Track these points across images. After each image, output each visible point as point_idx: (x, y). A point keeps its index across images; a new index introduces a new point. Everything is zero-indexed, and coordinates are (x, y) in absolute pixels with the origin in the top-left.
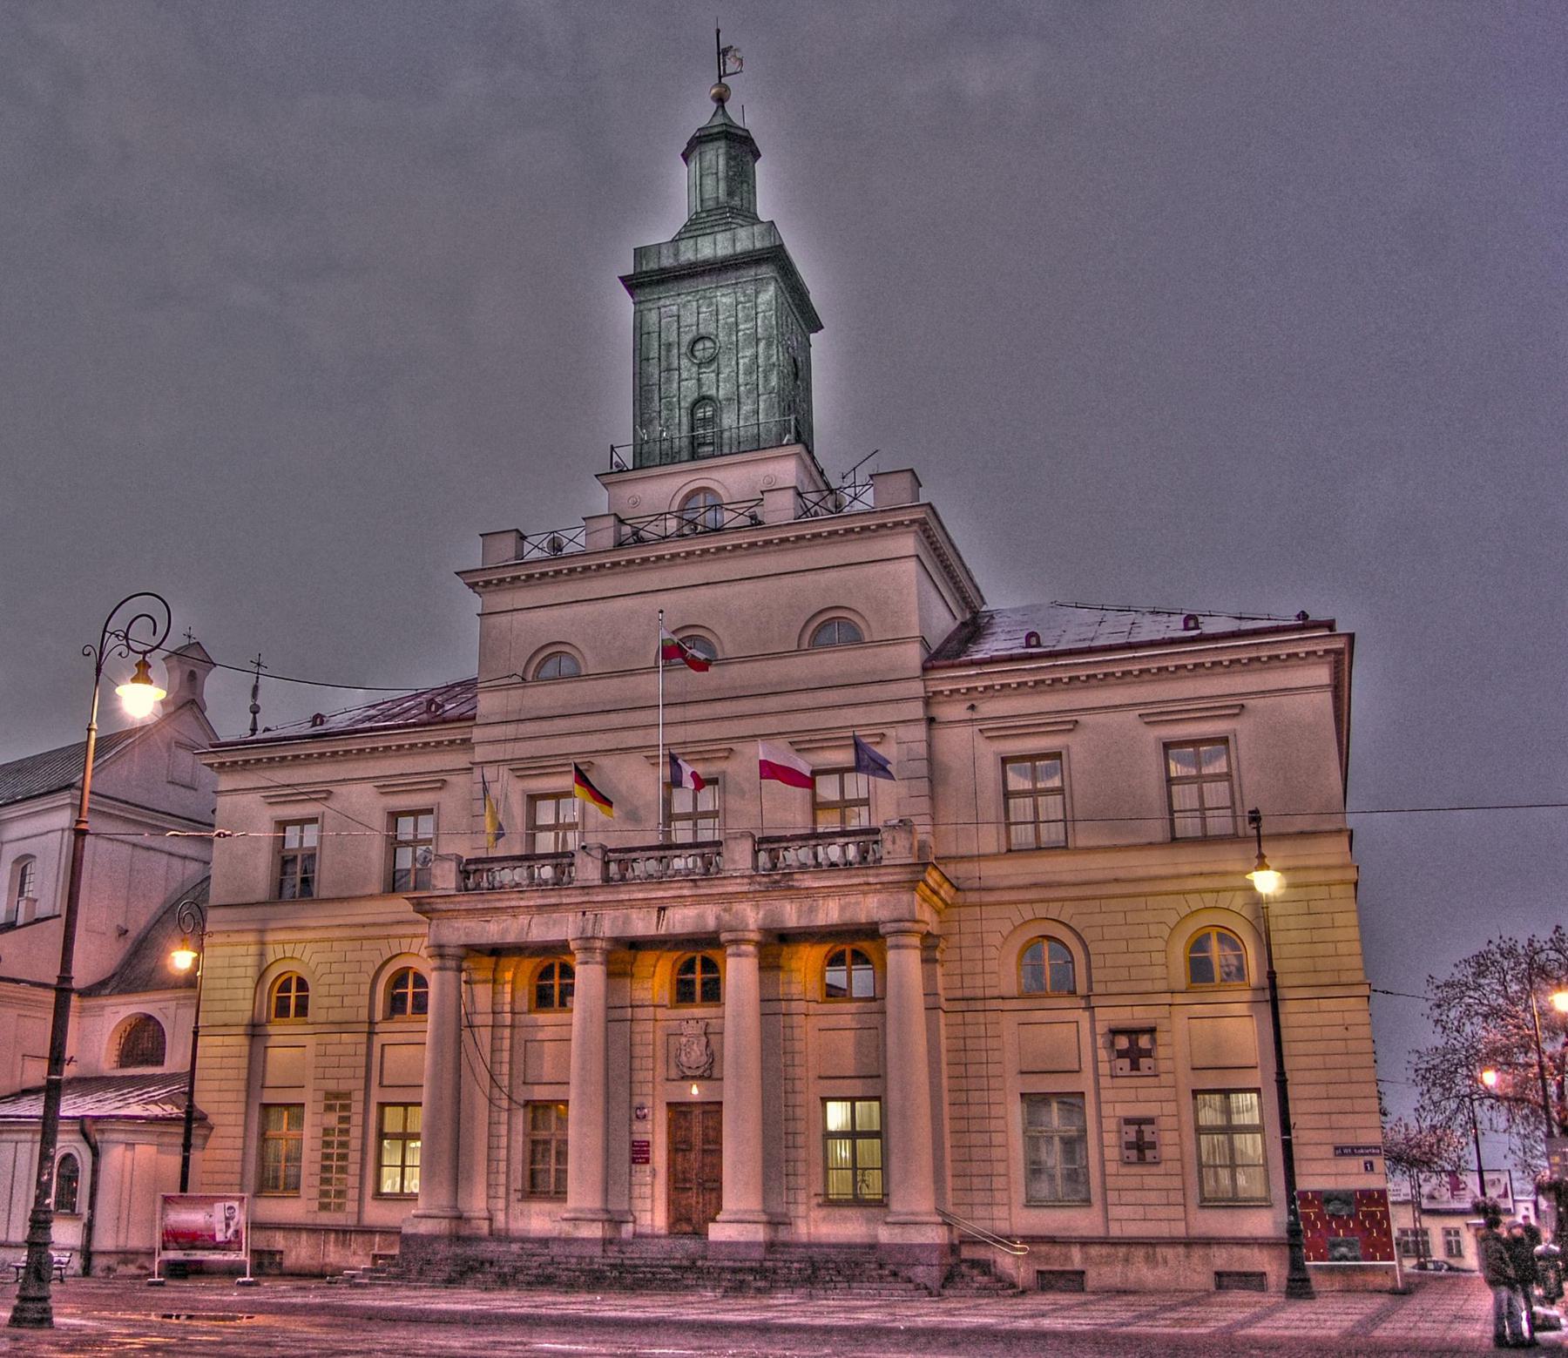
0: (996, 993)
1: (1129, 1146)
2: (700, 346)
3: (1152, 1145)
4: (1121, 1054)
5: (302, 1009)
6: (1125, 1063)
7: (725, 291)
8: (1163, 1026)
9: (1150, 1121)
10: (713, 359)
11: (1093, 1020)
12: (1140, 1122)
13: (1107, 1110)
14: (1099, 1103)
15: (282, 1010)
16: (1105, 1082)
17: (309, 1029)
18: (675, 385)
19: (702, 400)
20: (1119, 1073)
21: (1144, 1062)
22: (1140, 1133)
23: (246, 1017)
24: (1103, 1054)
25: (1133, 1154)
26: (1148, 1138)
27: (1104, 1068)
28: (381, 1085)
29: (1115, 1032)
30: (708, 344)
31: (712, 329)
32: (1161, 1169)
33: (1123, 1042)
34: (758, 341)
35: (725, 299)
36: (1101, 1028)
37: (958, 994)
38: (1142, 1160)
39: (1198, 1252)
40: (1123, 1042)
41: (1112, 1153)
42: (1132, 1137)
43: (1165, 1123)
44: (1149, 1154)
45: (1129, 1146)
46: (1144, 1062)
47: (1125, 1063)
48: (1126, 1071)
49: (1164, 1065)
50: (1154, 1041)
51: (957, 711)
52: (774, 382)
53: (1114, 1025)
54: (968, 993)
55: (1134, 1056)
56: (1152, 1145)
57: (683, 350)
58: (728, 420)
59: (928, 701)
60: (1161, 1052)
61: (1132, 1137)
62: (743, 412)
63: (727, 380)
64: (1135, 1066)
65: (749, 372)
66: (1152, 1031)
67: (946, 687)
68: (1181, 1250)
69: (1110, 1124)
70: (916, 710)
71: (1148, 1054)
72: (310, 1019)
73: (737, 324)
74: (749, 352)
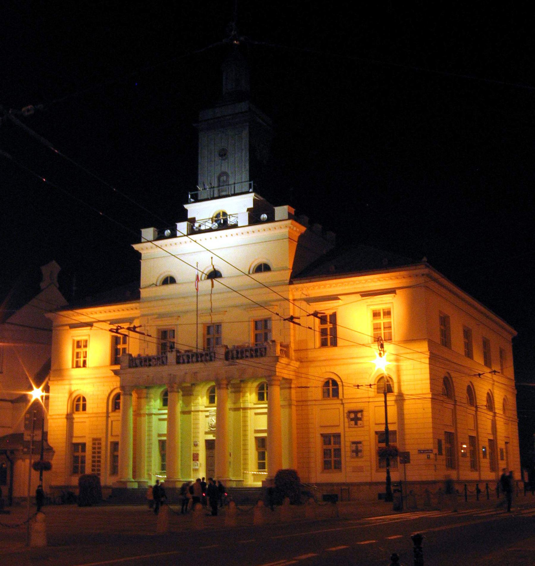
1: (353, 451)
3: (361, 451)
4: (352, 420)
5: (84, 409)
9: (360, 443)
11: (344, 407)
13: (347, 439)
14: (345, 437)
15: (77, 409)
16: (347, 429)
17: (87, 416)
22: (357, 447)
23: (65, 413)
24: (346, 420)
26: (360, 448)
27: (347, 425)
28: (112, 435)
29: (350, 412)
32: (362, 459)
33: (352, 416)
34: (242, 150)
36: (346, 411)
37: (300, 399)
41: (349, 454)
43: (365, 443)
44: (360, 454)
45: (353, 451)
48: (353, 426)
49: (366, 423)
50: (362, 415)
54: (303, 399)
60: (365, 418)
61: (354, 448)
64: (356, 424)
66: (361, 411)
69: (348, 444)
71: (360, 419)
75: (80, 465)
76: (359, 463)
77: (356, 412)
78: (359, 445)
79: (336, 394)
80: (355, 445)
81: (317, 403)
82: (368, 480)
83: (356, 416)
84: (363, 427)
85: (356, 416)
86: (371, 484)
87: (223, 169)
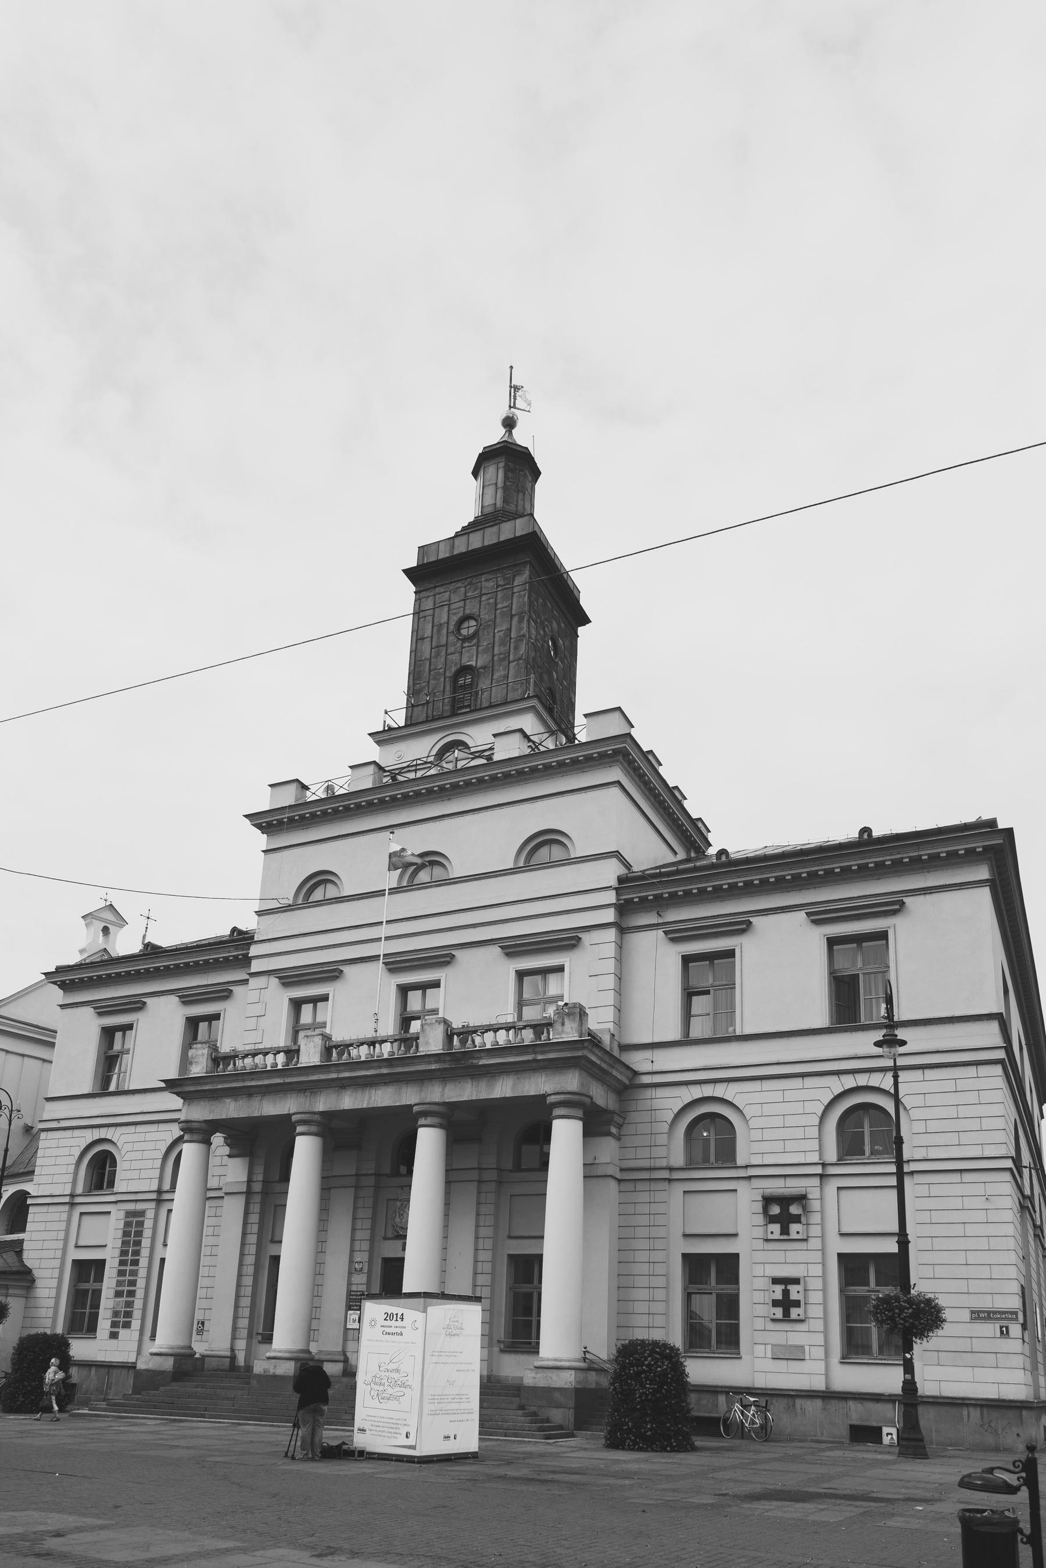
0: (663, 1163)
1: (775, 1303)
2: (466, 625)
3: (797, 1304)
4: (772, 1219)
5: (111, 1184)
6: (776, 1228)
7: (489, 576)
8: (814, 1194)
9: (796, 1281)
10: (475, 634)
12: (786, 1281)
18: (443, 659)
19: (465, 670)
20: (770, 1237)
21: (794, 1228)
22: (786, 1293)
25: (779, 1312)
26: (794, 1296)
29: (768, 1200)
30: (473, 623)
31: (476, 610)
33: (775, 1210)
34: (512, 616)
35: (488, 584)
38: (786, 1317)
39: (834, 1405)
40: (775, 1210)
42: (778, 1296)
44: (794, 1313)
45: (775, 1303)
46: (794, 1228)
47: (776, 1228)
48: (777, 1235)
50: (804, 1208)
51: (651, 919)
52: (522, 650)
53: (768, 1192)
55: (785, 1221)
56: (797, 1304)
57: (451, 627)
58: (484, 684)
62: (495, 677)
63: (485, 651)
64: (785, 1231)
65: (503, 643)
66: (801, 1199)
67: (635, 896)
68: (819, 1403)
69: (764, 1283)
70: (609, 916)
71: (797, 1219)
72: (115, 1190)
73: (496, 604)
74: (505, 626)
75: (87, 1311)
76: (795, 1336)
77: (785, 1201)
78: (793, 1289)
79: (725, 1152)
80: (783, 1287)
81: (676, 1175)
82: (819, 1384)
83: (785, 1209)
84: (805, 1240)
85: (785, 1209)
86: (828, 1396)
87: (465, 661)
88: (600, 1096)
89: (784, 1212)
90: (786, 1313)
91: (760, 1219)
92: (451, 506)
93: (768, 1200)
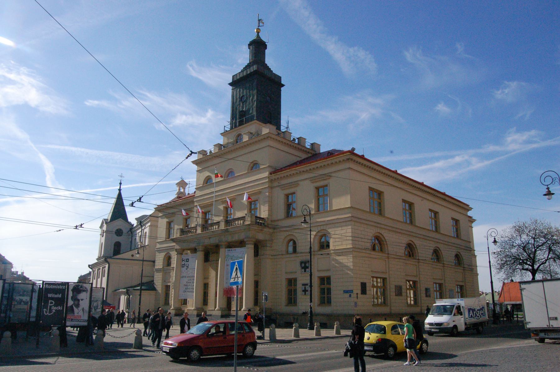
1: (303, 291)
6: (303, 270)
22: (305, 288)
33: (303, 265)
40: (303, 265)
45: (303, 291)
59: (271, 181)
69: (301, 285)
77: (305, 263)
88: (260, 236)
89: (305, 266)
90: (305, 294)
91: (300, 268)
92: (242, 58)
93: (301, 263)
